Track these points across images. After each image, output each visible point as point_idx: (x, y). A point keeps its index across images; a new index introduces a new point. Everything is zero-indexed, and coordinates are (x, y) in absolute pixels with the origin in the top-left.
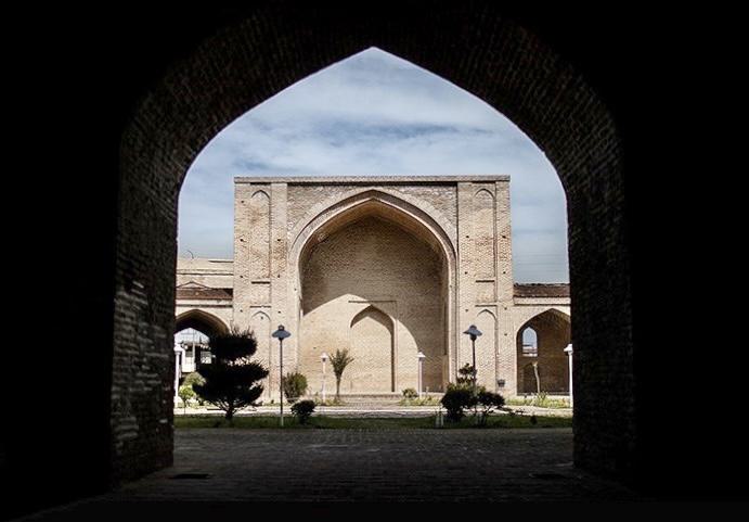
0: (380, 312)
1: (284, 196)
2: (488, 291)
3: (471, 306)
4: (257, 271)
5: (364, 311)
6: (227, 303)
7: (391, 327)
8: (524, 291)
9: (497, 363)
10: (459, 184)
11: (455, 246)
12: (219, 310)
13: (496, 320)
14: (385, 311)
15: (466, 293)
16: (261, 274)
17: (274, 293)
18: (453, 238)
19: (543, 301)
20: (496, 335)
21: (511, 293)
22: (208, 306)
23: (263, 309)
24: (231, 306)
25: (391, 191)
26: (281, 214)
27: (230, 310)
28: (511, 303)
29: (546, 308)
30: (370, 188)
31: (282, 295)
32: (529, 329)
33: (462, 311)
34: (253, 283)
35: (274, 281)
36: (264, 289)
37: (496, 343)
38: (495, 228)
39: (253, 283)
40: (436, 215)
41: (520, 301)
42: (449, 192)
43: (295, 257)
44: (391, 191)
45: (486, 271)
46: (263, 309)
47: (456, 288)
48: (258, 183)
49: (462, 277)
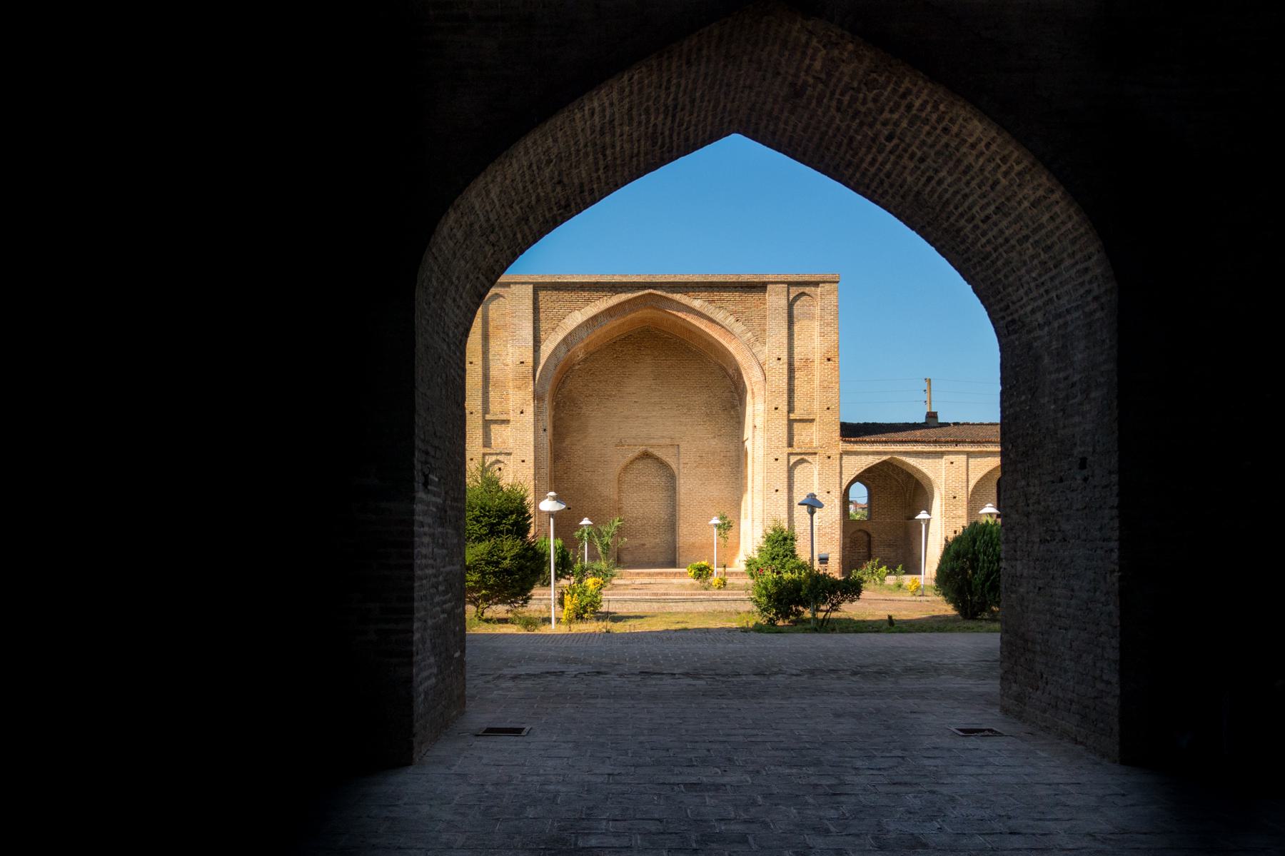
0: (657, 459)
5: (632, 462)
7: (672, 478)
8: (851, 431)
10: (769, 287)
14: (664, 458)
19: (880, 448)
29: (885, 458)
32: (858, 484)
41: (850, 447)
42: (752, 298)
44: (670, 295)
46: (499, 458)
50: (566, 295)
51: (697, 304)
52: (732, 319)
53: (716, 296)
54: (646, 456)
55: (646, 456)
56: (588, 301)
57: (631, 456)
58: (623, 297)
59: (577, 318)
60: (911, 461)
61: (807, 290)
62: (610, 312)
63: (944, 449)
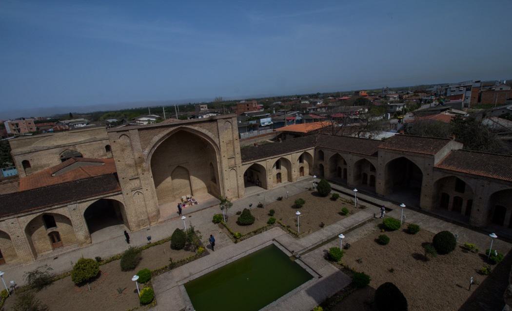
0: (183, 167)
1: (137, 136)
2: (232, 162)
4: (131, 173)
6: (120, 192)
7: (187, 170)
9: (238, 187)
11: (219, 146)
12: (115, 197)
16: (133, 174)
17: (143, 182)
18: (217, 142)
20: (237, 177)
21: (241, 161)
22: (110, 196)
23: (138, 191)
24: (121, 193)
25: (187, 126)
26: (137, 144)
27: (121, 195)
30: (179, 126)
34: (130, 180)
35: (141, 176)
36: (137, 181)
37: (237, 180)
38: (233, 136)
39: (130, 180)
40: (209, 134)
41: (244, 163)
42: (214, 125)
43: (147, 165)
44: (187, 126)
45: (231, 153)
46: (138, 191)
47: (221, 163)
49: (223, 159)
50: (152, 131)
53: (202, 125)
54: (179, 166)
56: (159, 132)
57: (174, 168)
59: (156, 138)
60: (259, 163)
61: (228, 120)
62: (168, 134)
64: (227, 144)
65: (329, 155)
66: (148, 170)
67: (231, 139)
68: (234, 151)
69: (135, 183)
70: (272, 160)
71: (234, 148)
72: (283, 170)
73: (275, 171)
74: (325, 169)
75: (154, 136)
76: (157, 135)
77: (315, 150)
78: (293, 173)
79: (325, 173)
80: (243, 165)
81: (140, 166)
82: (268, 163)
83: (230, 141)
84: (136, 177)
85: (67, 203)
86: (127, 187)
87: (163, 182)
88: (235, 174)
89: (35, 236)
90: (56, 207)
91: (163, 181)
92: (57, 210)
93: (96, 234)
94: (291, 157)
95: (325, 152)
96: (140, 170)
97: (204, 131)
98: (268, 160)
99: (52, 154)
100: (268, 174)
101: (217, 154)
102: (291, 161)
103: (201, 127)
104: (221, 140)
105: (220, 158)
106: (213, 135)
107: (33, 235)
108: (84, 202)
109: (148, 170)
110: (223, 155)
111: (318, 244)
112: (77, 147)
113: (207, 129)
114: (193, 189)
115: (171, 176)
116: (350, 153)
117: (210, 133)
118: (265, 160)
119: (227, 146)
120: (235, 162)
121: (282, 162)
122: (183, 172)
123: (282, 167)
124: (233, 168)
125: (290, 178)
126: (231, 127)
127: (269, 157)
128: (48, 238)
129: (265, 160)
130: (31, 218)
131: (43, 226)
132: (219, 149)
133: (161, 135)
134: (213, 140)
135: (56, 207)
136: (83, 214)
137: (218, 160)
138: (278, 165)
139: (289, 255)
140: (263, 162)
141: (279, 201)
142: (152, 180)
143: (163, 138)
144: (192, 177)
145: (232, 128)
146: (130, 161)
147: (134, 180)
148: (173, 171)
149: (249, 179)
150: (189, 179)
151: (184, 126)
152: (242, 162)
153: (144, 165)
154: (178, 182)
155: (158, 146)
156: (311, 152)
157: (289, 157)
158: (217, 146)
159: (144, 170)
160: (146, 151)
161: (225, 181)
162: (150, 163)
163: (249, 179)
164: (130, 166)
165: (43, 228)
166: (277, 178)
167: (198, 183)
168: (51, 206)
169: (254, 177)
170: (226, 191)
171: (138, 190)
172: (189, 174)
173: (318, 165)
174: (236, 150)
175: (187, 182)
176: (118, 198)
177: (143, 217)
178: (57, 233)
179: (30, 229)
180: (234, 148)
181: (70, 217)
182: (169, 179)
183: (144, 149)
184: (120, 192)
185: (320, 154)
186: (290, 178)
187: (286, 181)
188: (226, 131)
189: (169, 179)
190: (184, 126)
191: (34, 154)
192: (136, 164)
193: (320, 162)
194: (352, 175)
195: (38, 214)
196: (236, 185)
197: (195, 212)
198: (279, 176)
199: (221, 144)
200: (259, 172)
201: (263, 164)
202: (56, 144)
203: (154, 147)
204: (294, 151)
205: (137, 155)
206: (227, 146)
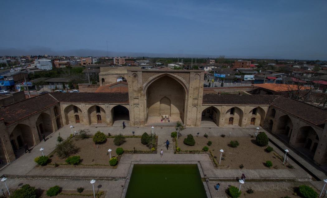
0: (168, 98)
1: (141, 75)
2: (196, 102)
3: (191, 105)
4: (135, 95)
6: (128, 104)
10: (191, 73)
11: (188, 89)
13: (197, 109)
15: (190, 101)
16: (136, 96)
18: (188, 87)
20: (197, 112)
21: (202, 102)
22: (124, 105)
23: (137, 105)
24: (129, 105)
25: (170, 74)
26: (141, 81)
27: (128, 106)
28: (201, 105)
31: (142, 102)
33: (189, 106)
35: (140, 98)
36: (137, 100)
37: (197, 114)
38: (199, 85)
40: (184, 81)
41: (204, 104)
42: (187, 75)
43: (144, 92)
44: (170, 74)
45: (196, 96)
46: (137, 105)
48: (133, 71)
49: (189, 98)
50: (149, 74)
51: (175, 76)
52: (182, 79)
53: (180, 74)
55: (165, 97)
58: (162, 74)
59: (151, 78)
60: (216, 107)
61: (198, 73)
62: (158, 77)
63: (222, 105)
64: (194, 89)
65: (279, 114)
66: (144, 96)
67: (198, 86)
68: (198, 95)
69: (136, 101)
70: (227, 107)
71: (198, 93)
72: (236, 116)
73: (229, 115)
74: (273, 124)
75: (151, 76)
76: (152, 76)
77: (269, 107)
78: (243, 120)
79: (273, 128)
80: (203, 105)
81: (140, 92)
82: (224, 109)
83: (197, 87)
84: (137, 98)
85: (104, 103)
86: (132, 102)
87: (155, 104)
88: (196, 110)
89: (92, 114)
90: (100, 103)
91: (155, 103)
92: (101, 105)
93: (116, 122)
94: (244, 108)
95: (277, 111)
96: (139, 95)
97: (180, 78)
98: (223, 106)
99: (114, 77)
100: (221, 116)
101: (186, 94)
102: (243, 111)
103: (179, 75)
104: (191, 86)
105: (188, 97)
106: (186, 82)
107: (91, 114)
108: (111, 104)
109: (144, 96)
110: (190, 96)
111: (229, 179)
112: (125, 76)
113: (183, 78)
114: (171, 112)
115: (160, 102)
116: (298, 118)
117: (184, 80)
118: (222, 106)
119: (194, 91)
120: (198, 102)
121: (236, 110)
122: (166, 100)
123: (235, 114)
124: (195, 105)
125: (240, 124)
126: (199, 78)
127: (225, 104)
128: (96, 117)
129: (222, 106)
130: (90, 106)
131: (95, 111)
132: (188, 92)
133: (154, 77)
134: (183, 83)
135: (100, 103)
136: (111, 110)
137: (186, 98)
138: (232, 111)
139: (202, 176)
140: (218, 107)
141: (222, 138)
142: (146, 101)
143: (155, 78)
144: (172, 105)
145: (200, 79)
146: (136, 89)
147: (136, 99)
148: (162, 99)
149: (210, 115)
150: (170, 106)
151: (168, 73)
152: (203, 103)
153: (142, 92)
154: (163, 106)
155: (152, 82)
156: (265, 108)
157: (242, 108)
158: (187, 89)
159: (141, 95)
160: (145, 85)
161: (188, 113)
162: (146, 91)
163: (210, 115)
164: (135, 91)
165: (95, 112)
166: (230, 121)
167: (175, 110)
168: (98, 103)
169: (210, 115)
170: (188, 119)
171: (137, 105)
172: (170, 102)
173: (269, 120)
174: (200, 94)
175: (169, 107)
176: (127, 107)
177: (137, 120)
178: (100, 116)
179: (90, 111)
180: (198, 93)
181: (105, 110)
182: (159, 103)
183: (143, 83)
184: (128, 104)
185: (273, 112)
186: (240, 124)
187: (237, 125)
188: (195, 81)
189: (159, 103)
190: (168, 73)
191: (108, 76)
192: (138, 91)
193: (271, 118)
194: (295, 137)
195: (93, 105)
196: (195, 117)
197: (165, 126)
198: (231, 120)
199: (190, 88)
200: (217, 113)
201: (219, 108)
202: (116, 72)
203: (149, 83)
204: (248, 104)
205: (139, 86)
206: (194, 91)
